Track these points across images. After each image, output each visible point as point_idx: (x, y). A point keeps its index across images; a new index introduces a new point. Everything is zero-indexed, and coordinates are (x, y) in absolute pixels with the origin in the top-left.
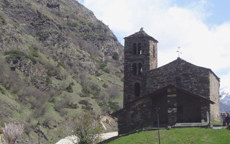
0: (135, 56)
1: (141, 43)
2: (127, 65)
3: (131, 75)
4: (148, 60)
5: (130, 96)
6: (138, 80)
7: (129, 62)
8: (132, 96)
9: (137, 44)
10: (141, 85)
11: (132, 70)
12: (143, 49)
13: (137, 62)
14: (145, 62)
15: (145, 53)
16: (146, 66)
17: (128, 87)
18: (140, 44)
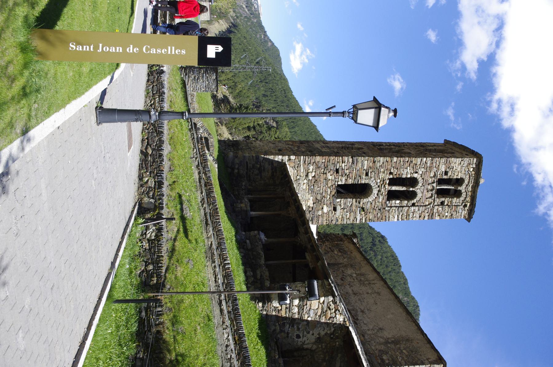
0: (435, 185)
1: (462, 199)
2: (416, 164)
3: (391, 173)
4: (420, 217)
5: (342, 175)
6: (378, 195)
7: (423, 170)
8: (341, 180)
9: (459, 188)
10: (365, 200)
11: (404, 176)
12: (446, 204)
13: (418, 189)
14: (417, 208)
15: (436, 207)
16: (408, 210)
17: (365, 168)
18: (458, 194)
